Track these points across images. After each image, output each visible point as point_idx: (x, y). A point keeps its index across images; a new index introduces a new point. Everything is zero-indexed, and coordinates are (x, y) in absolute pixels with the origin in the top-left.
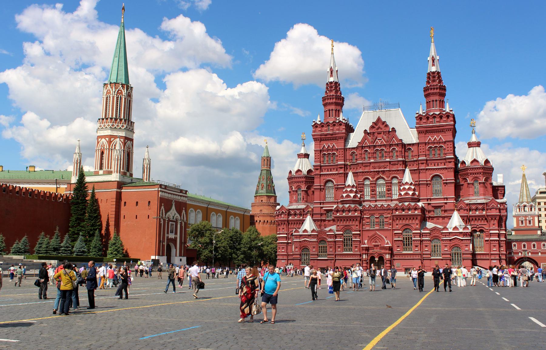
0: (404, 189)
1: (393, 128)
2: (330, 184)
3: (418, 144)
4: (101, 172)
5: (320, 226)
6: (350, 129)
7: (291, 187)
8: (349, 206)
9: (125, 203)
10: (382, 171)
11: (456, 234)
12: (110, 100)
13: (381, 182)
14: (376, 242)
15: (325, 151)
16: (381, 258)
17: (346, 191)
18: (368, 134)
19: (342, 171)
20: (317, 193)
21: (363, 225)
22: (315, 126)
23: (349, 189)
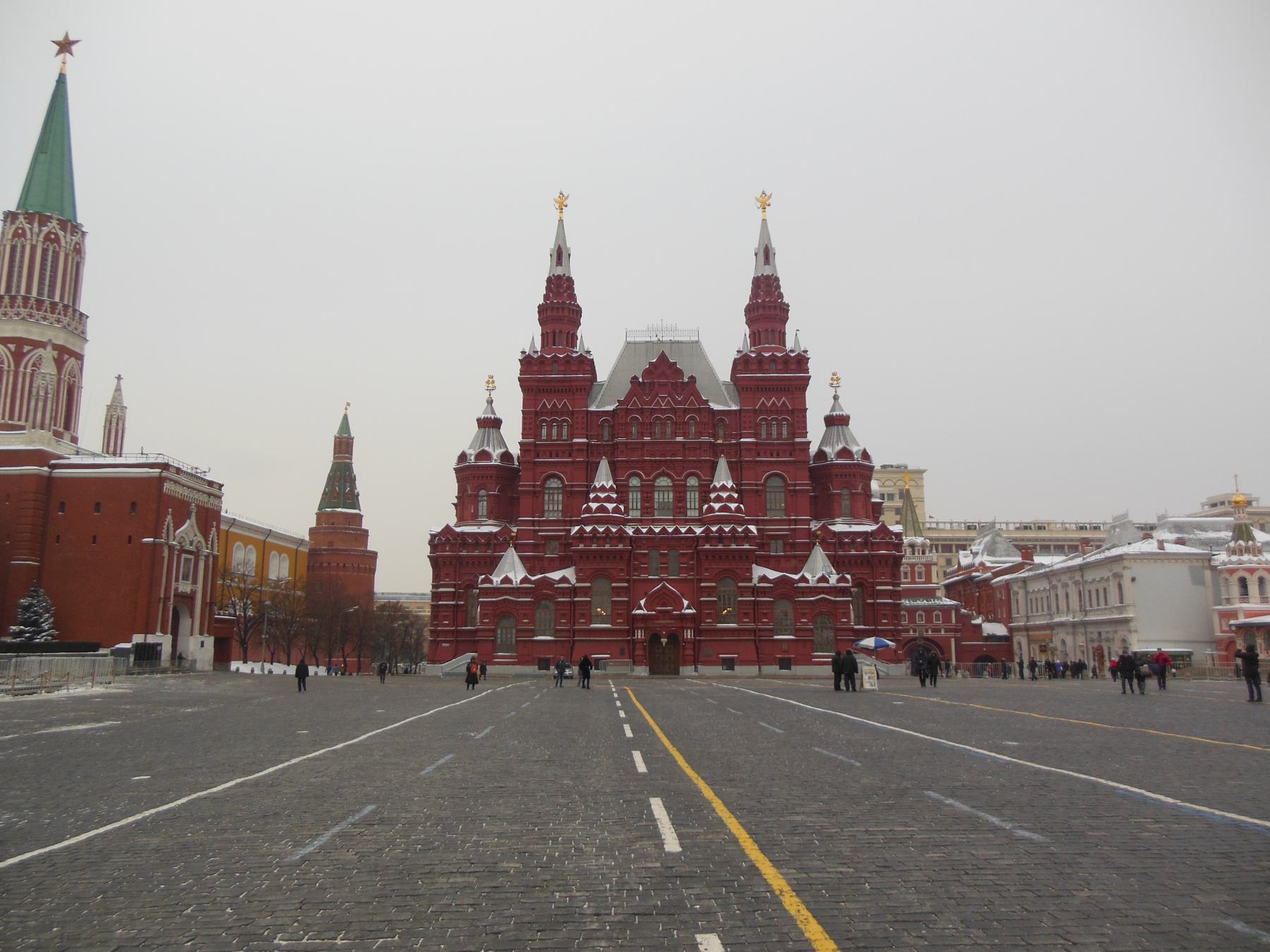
1: (692, 379)
2: (554, 483)
3: (740, 411)
5: (531, 571)
8: (608, 529)
11: (823, 590)
13: (664, 482)
14: (664, 605)
15: (547, 414)
16: (674, 638)
20: (525, 502)
21: (635, 570)
23: (602, 495)
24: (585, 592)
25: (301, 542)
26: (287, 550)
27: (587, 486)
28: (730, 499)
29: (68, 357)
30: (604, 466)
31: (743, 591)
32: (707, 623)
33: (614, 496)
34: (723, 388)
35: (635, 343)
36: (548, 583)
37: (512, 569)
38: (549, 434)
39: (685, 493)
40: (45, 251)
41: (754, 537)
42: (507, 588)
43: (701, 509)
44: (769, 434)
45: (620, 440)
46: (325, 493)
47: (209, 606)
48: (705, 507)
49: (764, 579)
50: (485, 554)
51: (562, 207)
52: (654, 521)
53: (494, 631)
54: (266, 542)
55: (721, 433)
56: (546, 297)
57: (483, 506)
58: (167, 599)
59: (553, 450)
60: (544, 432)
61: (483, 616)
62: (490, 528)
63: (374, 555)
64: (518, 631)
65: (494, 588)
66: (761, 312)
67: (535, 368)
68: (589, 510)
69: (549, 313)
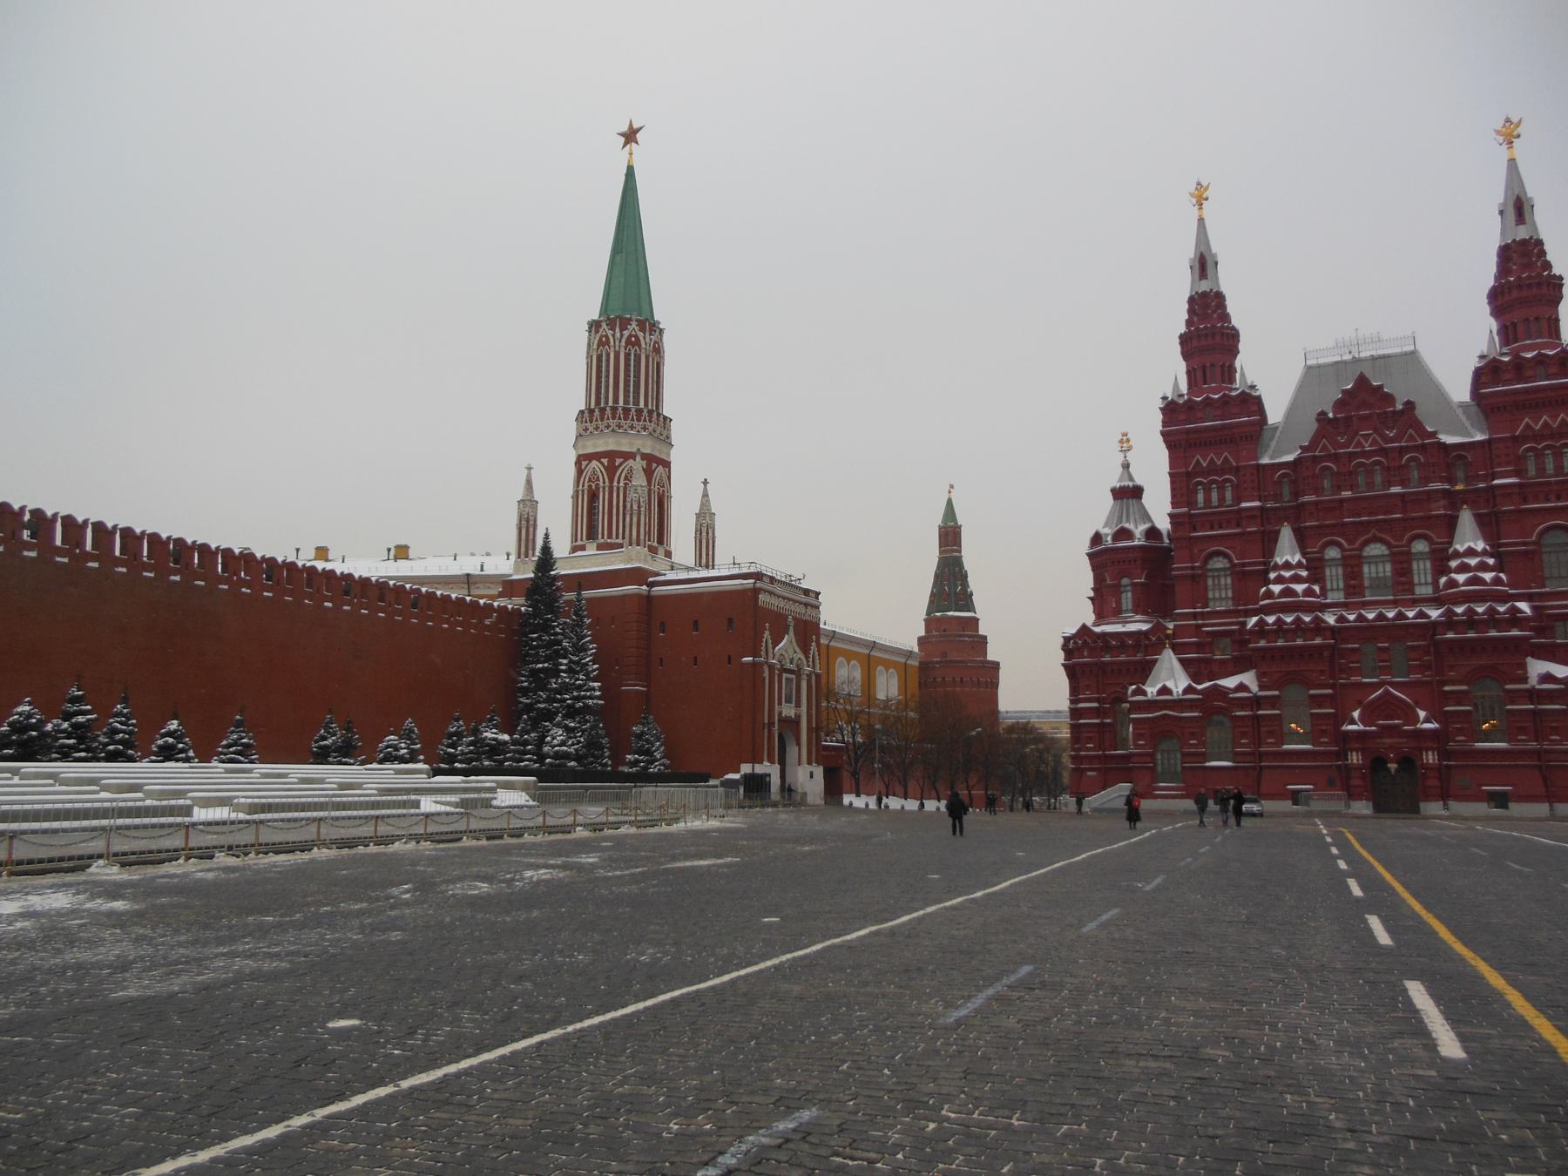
1: (1410, 405)
2: (1219, 563)
3: (1489, 442)
5: (1196, 678)
7: (1099, 579)
9: (663, 624)
10: (1378, 521)
12: (608, 360)
13: (1376, 549)
16: (1408, 763)
23: (1287, 574)
24: (1272, 702)
25: (910, 654)
26: (895, 665)
27: (1265, 564)
28: (1483, 567)
29: (657, 465)
30: (1286, 535)
31: (1514, 697)
32: (1458, 742)
33: (1304, 573)
34: (1459, 412)
35: (1319, 366)
36: (1222, 692)
37: (1170, 677)
38: (1208, 500)
39: (1409, 563)
40: (627, 355)
41: (1527, 619)
42: (1166, 700)
43: (1435, 583)
44: (1541, 470)
45: (1307, 498)
46: (932, 595)
47: (816, 731)
48: (1443, 580)
49: (1548, 678)
51: (1200, 199)
52: (1365, 605)
53: (1152, 756)
54: (870, 656)
55: (1460, 474)
56: (1189, 323)
57: (1127, 598)
58: (771, 724)
59: (1212, 520)
60: (1200, 497)
61: (1137, 736)
62: (1139, 625)
63: (995, 666)
64: (1184, 755)
65: (1149, 702)
66: (1515, 294)
67: (1182, 417)
68: (1269, 594)
69: (1195, 343)
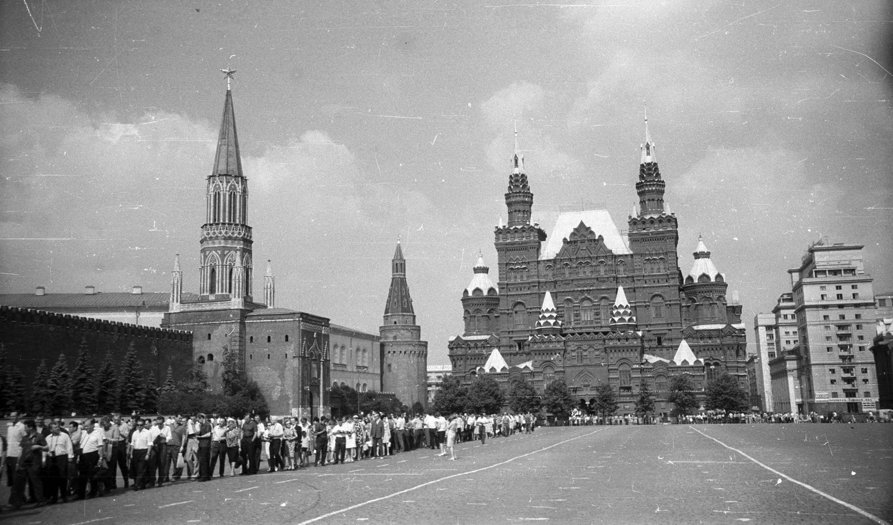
0: (618, 313)
3: (632, 255)
4: (212, 297)
6: (542, 236)
9: (252, 338)
13: (586, 304)
17: (544, 317)
18: (568, 243)
19: (535, 290)
22: (498, 232)
23: (547, 315)
50: (479, 353)
68: (539, 324)
